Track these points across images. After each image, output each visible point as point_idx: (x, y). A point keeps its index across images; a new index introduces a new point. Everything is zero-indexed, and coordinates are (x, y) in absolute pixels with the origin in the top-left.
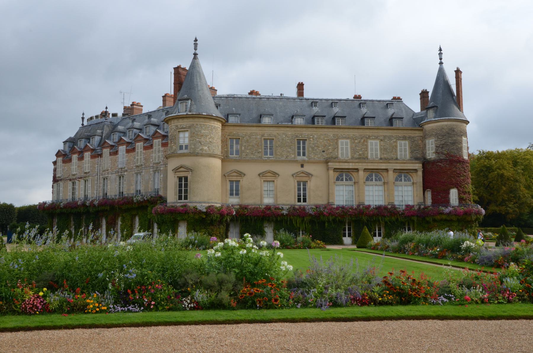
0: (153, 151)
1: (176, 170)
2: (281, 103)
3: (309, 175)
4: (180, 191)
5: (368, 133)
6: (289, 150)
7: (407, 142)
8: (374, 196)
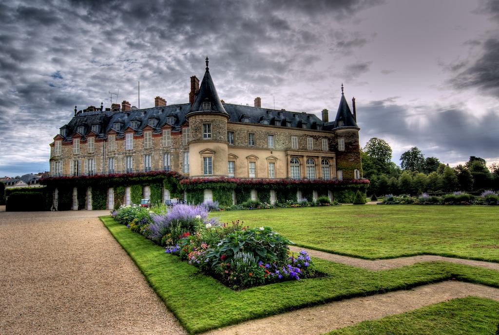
0: (162, 138)
1: (202, 152)
2: (249, 110)
3: (276, 159)
4: (205, 168)
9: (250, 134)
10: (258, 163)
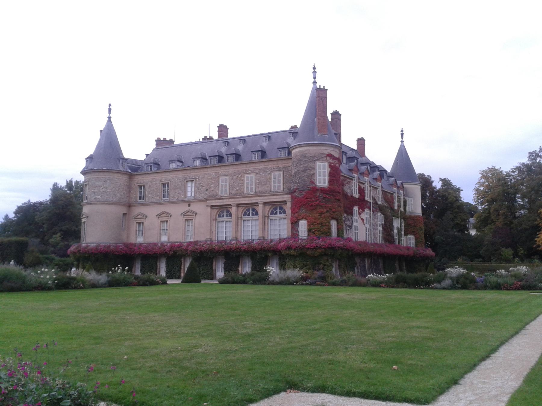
5: (244, 168)
6: (180, 191)
7: (281, 173)
8: (251, 231)
9: (164, 184)
10: (171, 221)
